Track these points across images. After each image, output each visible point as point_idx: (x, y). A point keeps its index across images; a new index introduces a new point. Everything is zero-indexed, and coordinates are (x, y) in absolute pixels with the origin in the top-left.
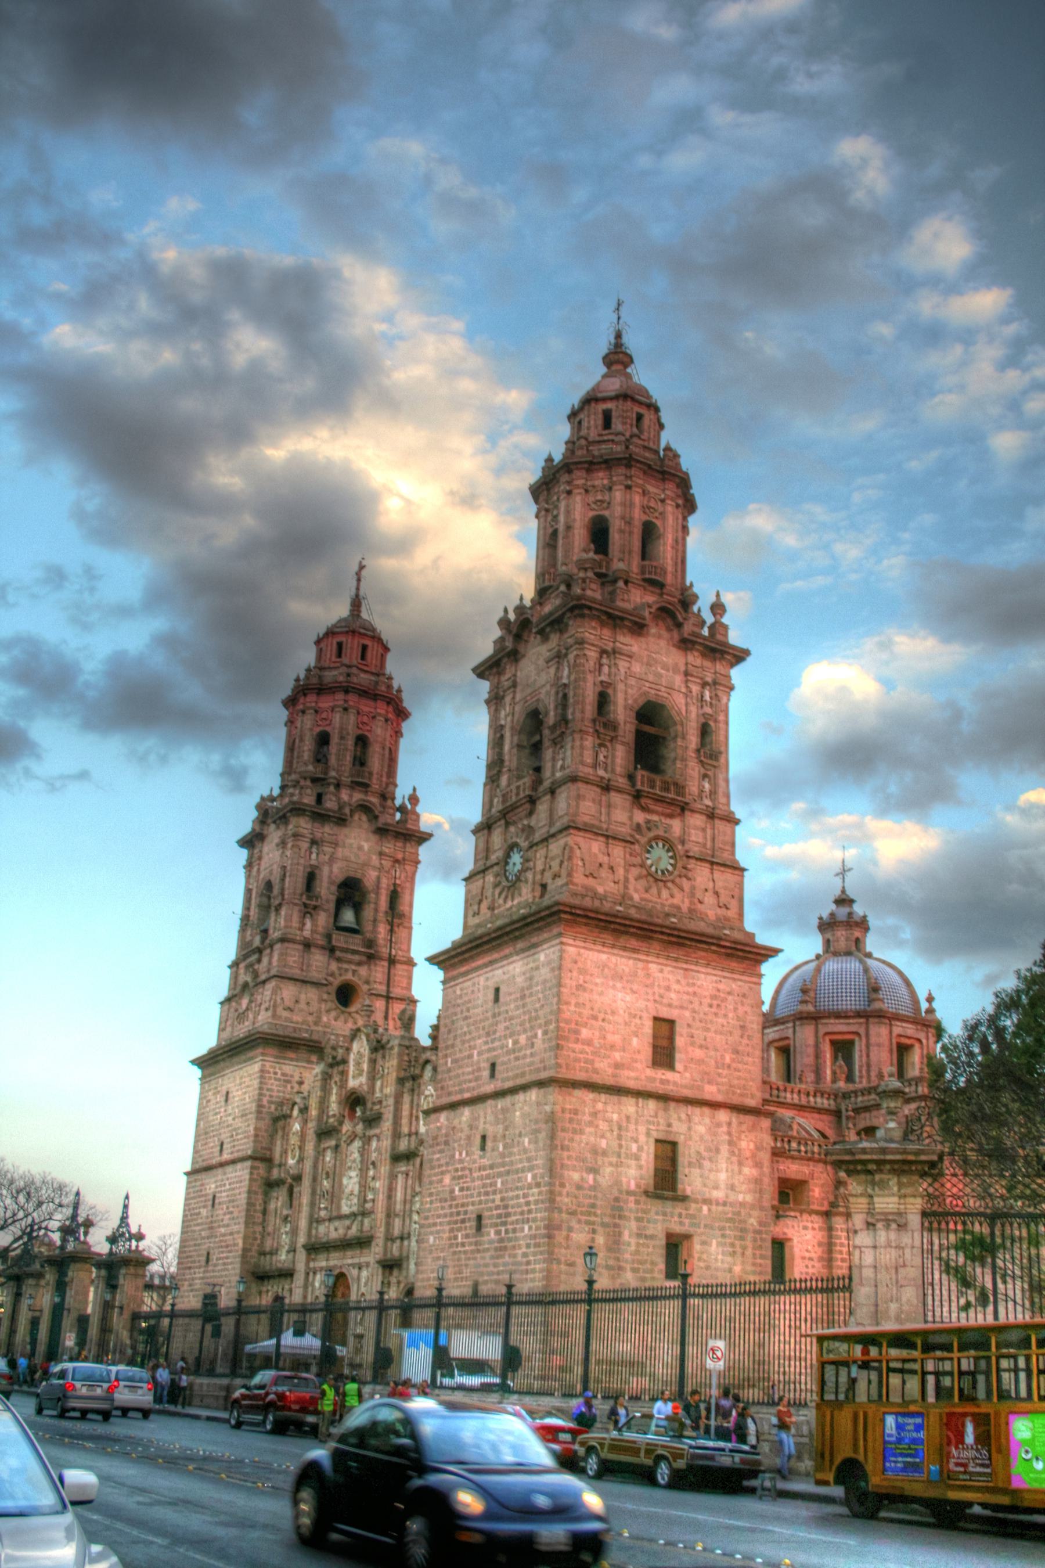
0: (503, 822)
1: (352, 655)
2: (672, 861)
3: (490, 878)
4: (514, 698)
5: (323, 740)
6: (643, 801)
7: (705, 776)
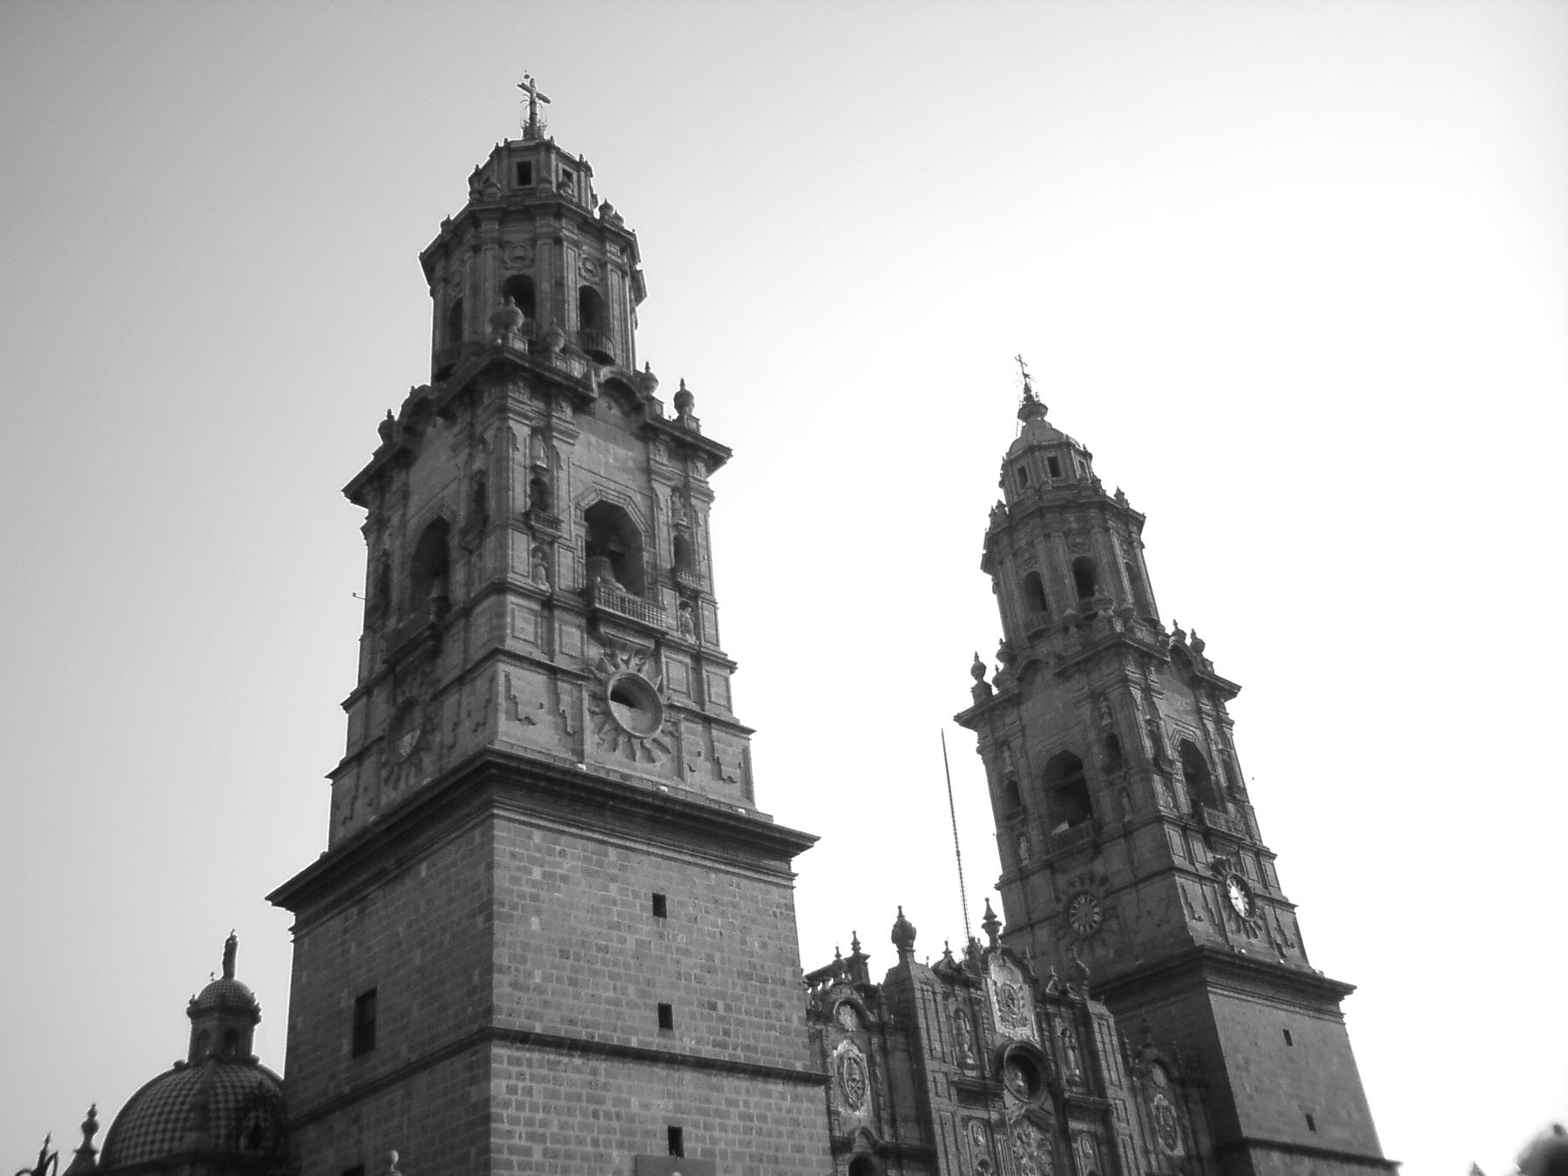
0: (391, 677)
3: (370, 763)
4: (404, 515)
7: (683, 606)
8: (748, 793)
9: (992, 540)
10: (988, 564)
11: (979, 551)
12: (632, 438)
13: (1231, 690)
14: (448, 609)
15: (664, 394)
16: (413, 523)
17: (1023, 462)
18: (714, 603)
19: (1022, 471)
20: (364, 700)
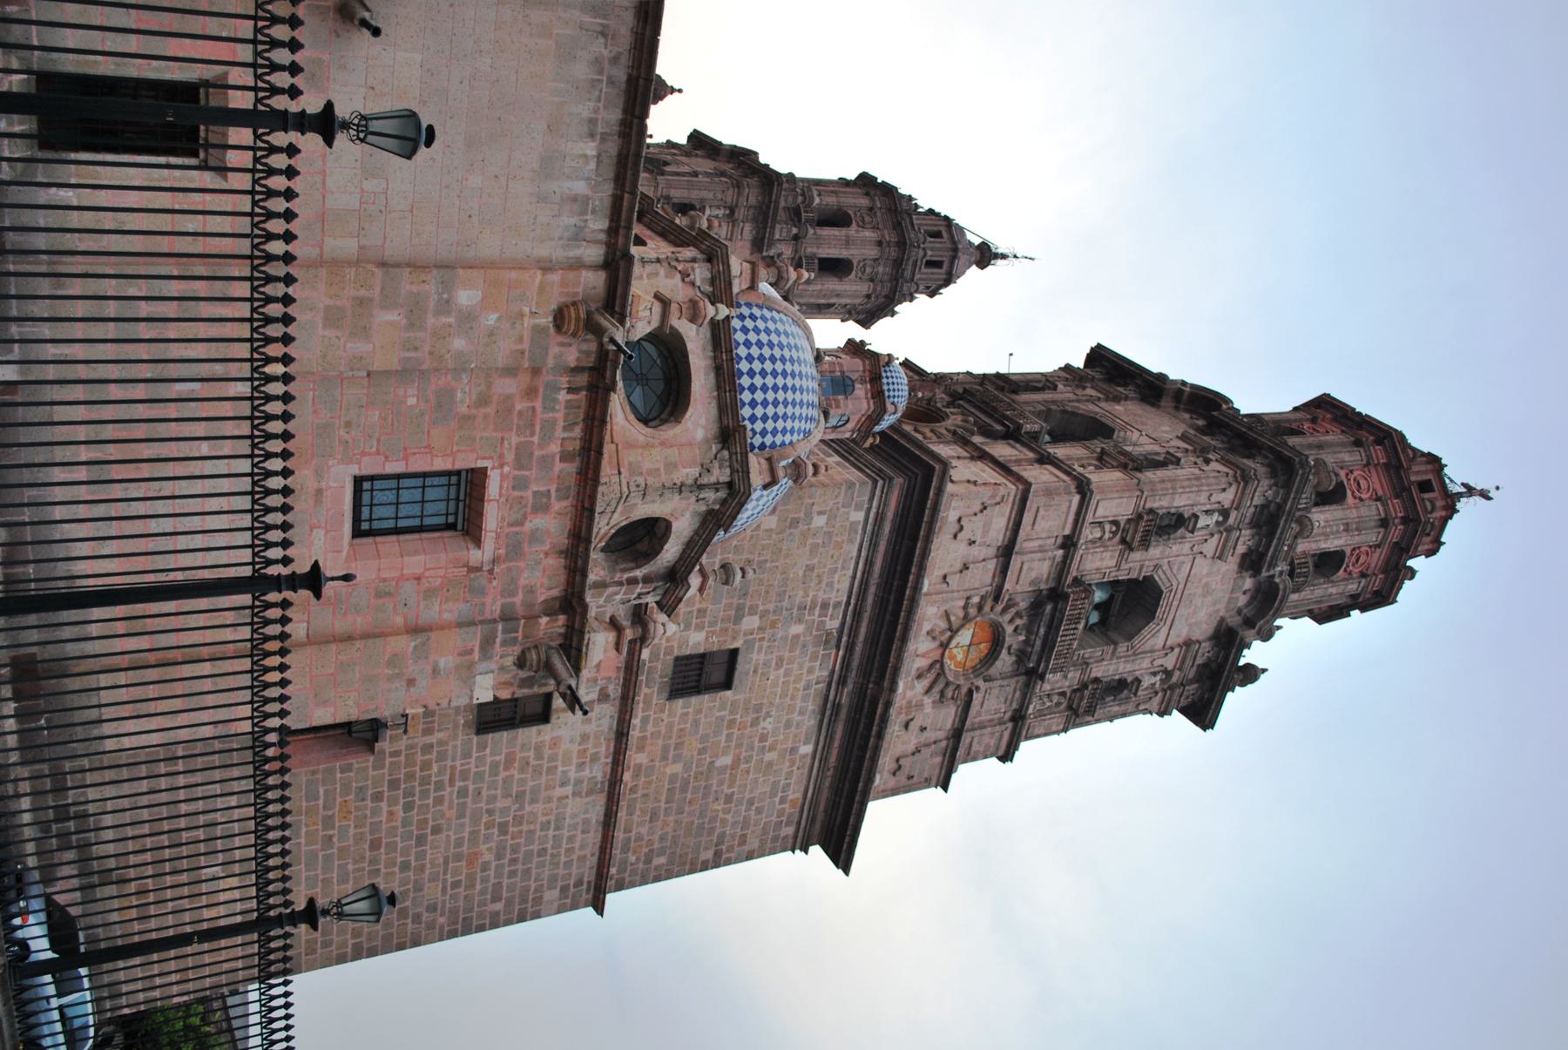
1: (934, 249)
4: (1099, 399)
5: (838, 219)
18: (1065, 730)
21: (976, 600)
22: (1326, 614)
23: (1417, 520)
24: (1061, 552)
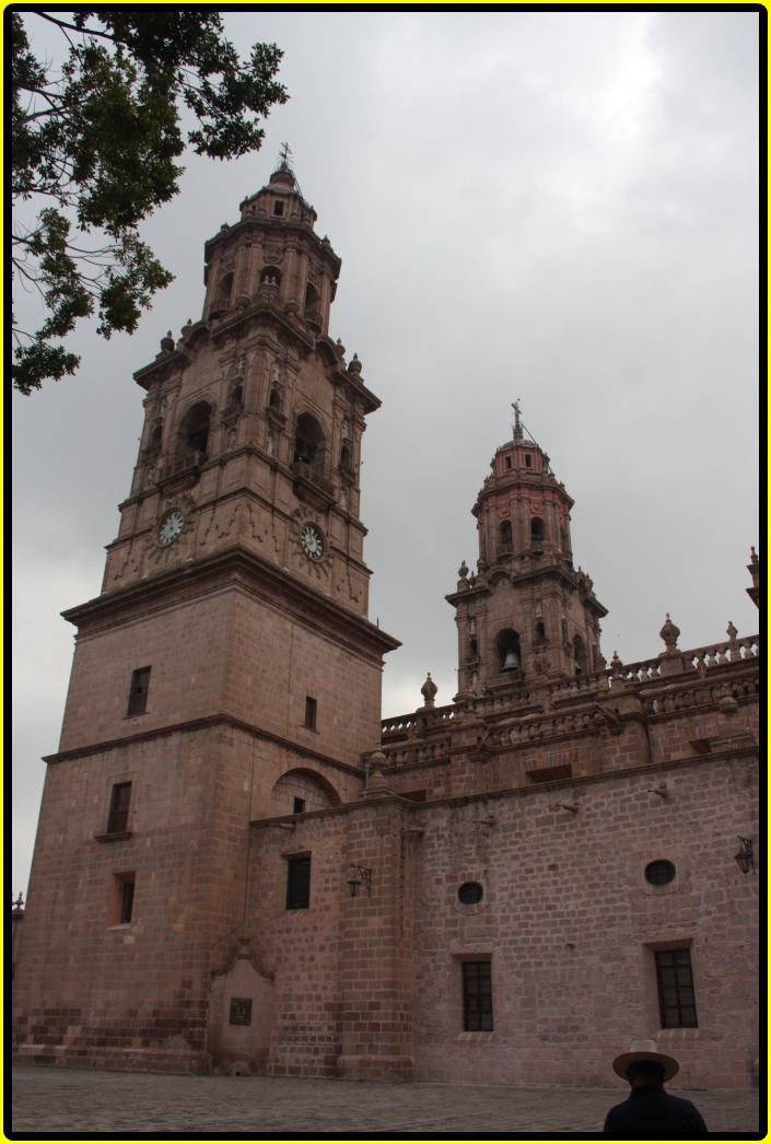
2: (320, 548)
3: (139, 544)
6: (300, 488)
8: (366, 610)
9: (484, 497)
10: (477, 511)
11: (474, 500)
12: (327, 382)
13: (602, 612)
14: (207, 459)
15: (348, 358)
16: (181, 404)
17: (511, 454)
18: (359, 492)
19: (508, 459)
20: (135, 506)
21: (292, 536)
22: (332, 299)
23: (304, 232)
24: (278, 475)
